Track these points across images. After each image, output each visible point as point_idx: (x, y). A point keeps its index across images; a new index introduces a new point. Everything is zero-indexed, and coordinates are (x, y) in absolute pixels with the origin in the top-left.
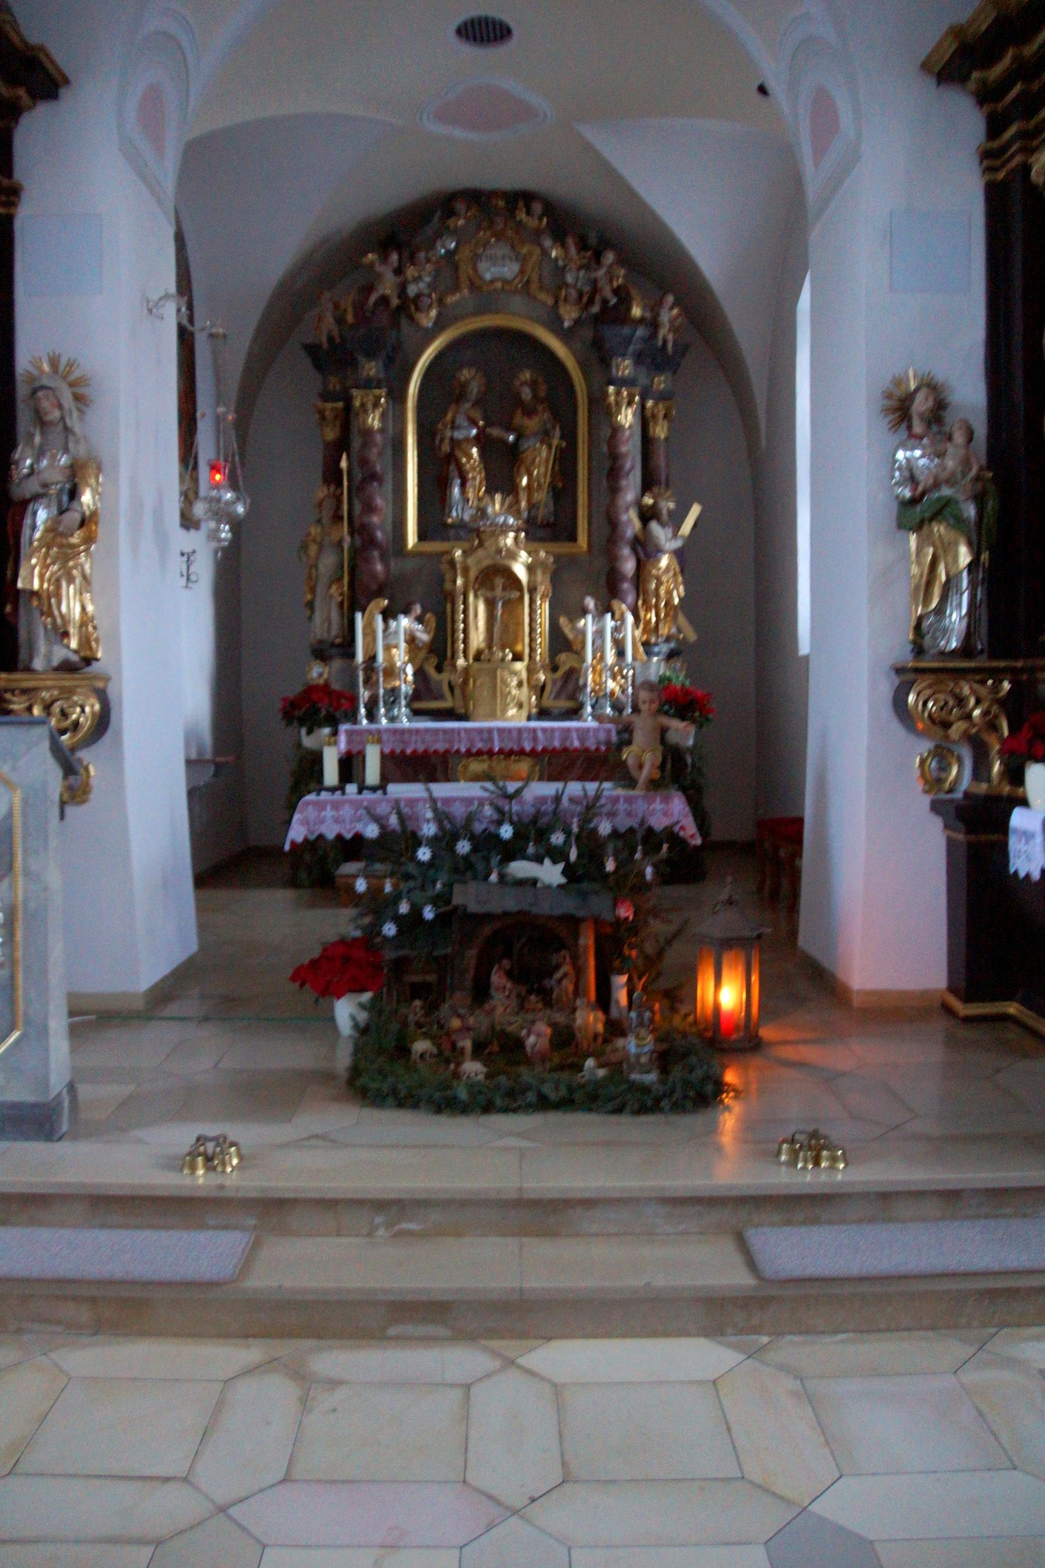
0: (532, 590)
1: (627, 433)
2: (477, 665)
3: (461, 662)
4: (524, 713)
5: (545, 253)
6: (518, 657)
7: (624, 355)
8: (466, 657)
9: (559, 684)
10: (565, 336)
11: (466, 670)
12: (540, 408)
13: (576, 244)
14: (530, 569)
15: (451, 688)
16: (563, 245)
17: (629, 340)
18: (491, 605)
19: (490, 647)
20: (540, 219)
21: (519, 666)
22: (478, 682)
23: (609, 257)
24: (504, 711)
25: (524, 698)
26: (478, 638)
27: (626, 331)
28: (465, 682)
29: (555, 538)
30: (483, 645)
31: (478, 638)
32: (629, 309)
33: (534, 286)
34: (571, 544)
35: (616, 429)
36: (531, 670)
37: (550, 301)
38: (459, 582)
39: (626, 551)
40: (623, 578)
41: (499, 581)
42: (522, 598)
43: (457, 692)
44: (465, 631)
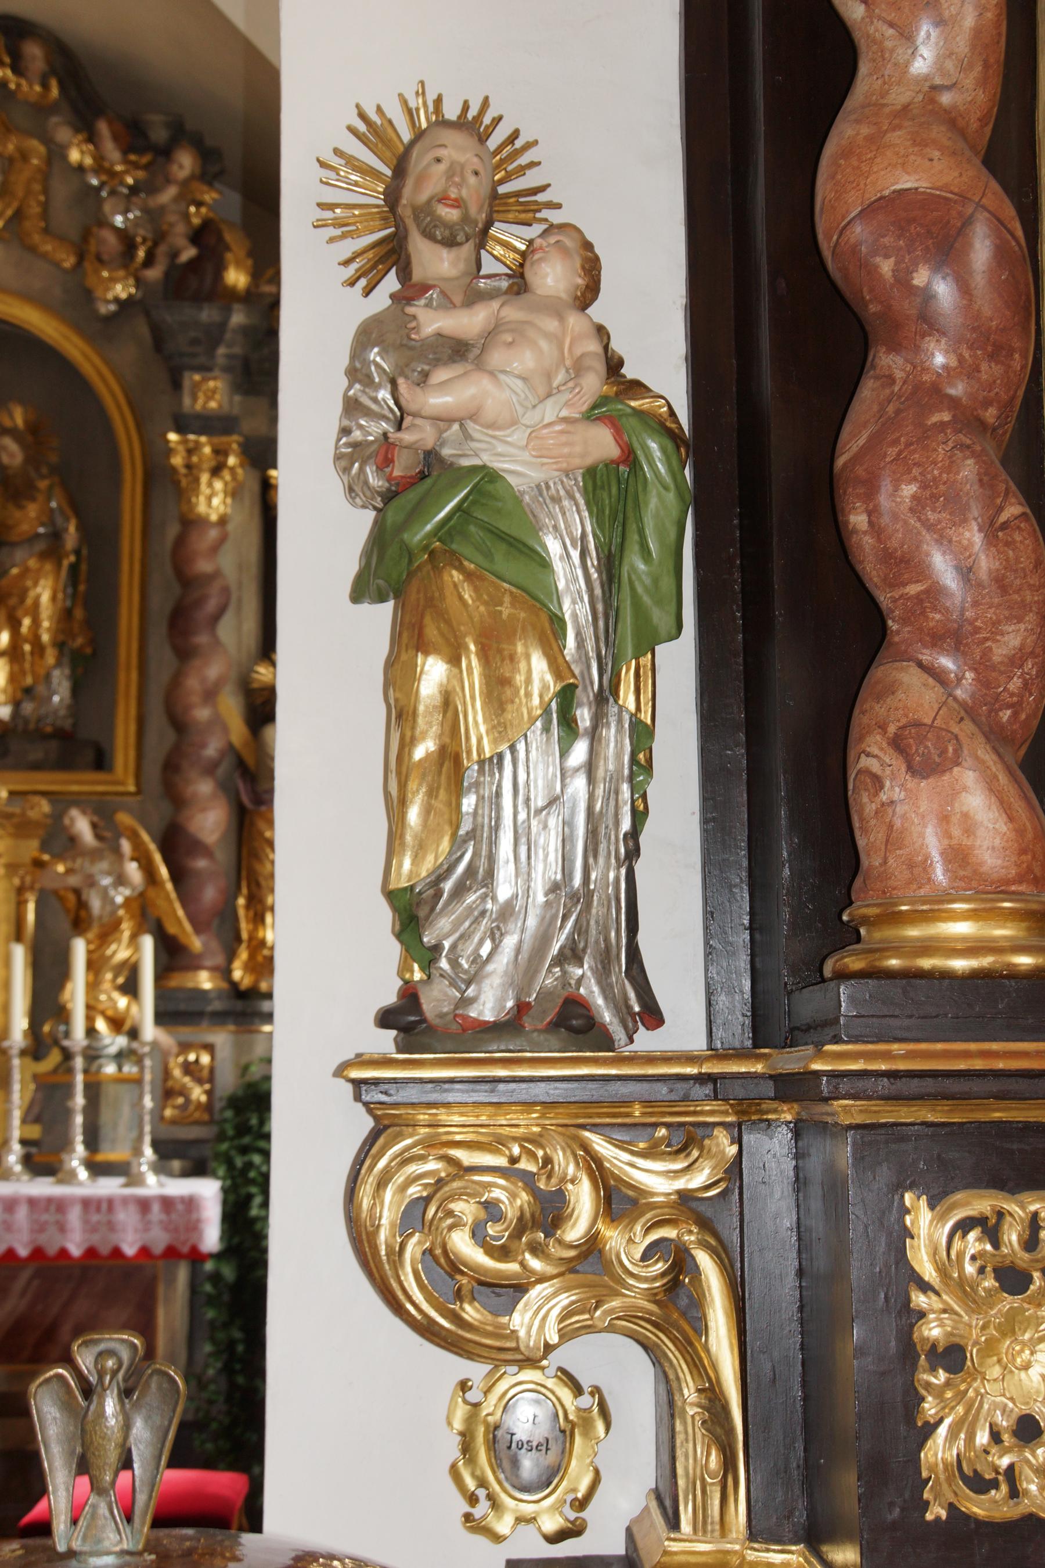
1: (213, 534)
5: (56, 154)
7: (205, 369)
10: (103, 329)
12: (43, 484)
13: (116, 138)
16: (92, 137)
17: (214, 335)
20: (45, 86)
23: (185, 163)
27: (208, 314)
29: (64, 763)
32: (220, 268)
33: (32, 225)
35: (191, 523)
37: (69, 262)
39: (204, 787)
40: (197, 847)
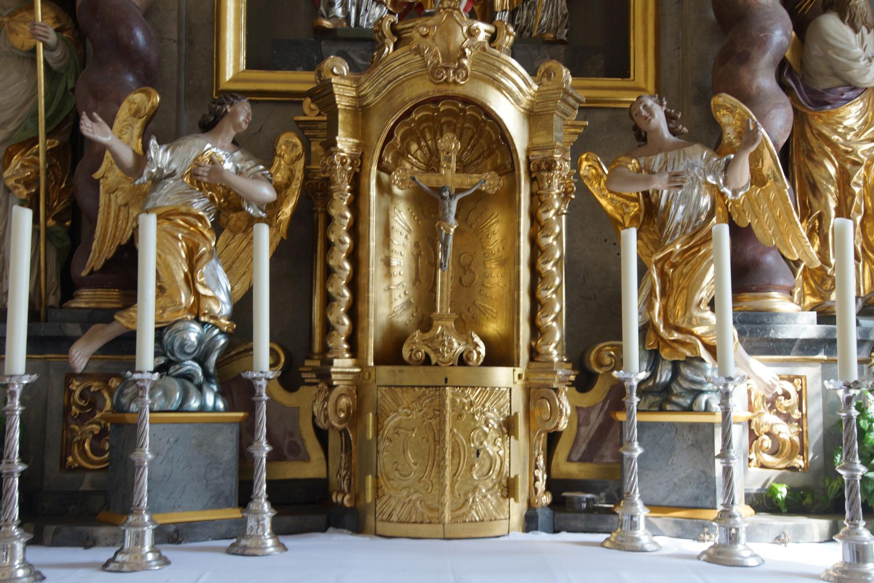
0: (539, 169)
2: (385, 373)
3: (343, 364)
4: (517, 509)
6: (500, 354)
8: (354, 349)
9: (595, 420)
11: (359, 386)
14: (534, 116)
15: (322, 436)
18: (427, 204)
19: (425, 323)
21: (503, 377)
22: (391, 422)
24: (462, 504)
25: (517, 469)
26: (390, 298)
28: (355, 416)
30: (403, 318)
31: (390, 298)
34: (618, 82)
36: (536, 394)
38: (345, 143)
41: (450, 144)
42: (513, 189)
43: (334, 441)
44: (356, 284)
